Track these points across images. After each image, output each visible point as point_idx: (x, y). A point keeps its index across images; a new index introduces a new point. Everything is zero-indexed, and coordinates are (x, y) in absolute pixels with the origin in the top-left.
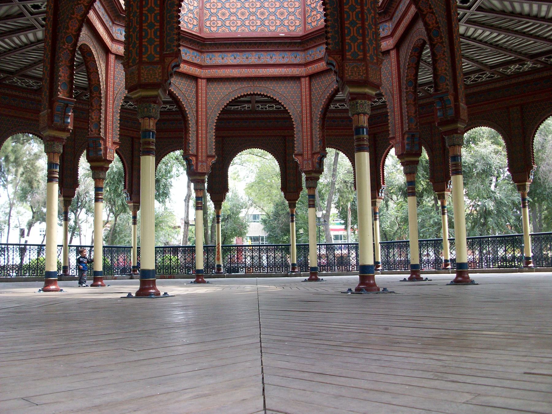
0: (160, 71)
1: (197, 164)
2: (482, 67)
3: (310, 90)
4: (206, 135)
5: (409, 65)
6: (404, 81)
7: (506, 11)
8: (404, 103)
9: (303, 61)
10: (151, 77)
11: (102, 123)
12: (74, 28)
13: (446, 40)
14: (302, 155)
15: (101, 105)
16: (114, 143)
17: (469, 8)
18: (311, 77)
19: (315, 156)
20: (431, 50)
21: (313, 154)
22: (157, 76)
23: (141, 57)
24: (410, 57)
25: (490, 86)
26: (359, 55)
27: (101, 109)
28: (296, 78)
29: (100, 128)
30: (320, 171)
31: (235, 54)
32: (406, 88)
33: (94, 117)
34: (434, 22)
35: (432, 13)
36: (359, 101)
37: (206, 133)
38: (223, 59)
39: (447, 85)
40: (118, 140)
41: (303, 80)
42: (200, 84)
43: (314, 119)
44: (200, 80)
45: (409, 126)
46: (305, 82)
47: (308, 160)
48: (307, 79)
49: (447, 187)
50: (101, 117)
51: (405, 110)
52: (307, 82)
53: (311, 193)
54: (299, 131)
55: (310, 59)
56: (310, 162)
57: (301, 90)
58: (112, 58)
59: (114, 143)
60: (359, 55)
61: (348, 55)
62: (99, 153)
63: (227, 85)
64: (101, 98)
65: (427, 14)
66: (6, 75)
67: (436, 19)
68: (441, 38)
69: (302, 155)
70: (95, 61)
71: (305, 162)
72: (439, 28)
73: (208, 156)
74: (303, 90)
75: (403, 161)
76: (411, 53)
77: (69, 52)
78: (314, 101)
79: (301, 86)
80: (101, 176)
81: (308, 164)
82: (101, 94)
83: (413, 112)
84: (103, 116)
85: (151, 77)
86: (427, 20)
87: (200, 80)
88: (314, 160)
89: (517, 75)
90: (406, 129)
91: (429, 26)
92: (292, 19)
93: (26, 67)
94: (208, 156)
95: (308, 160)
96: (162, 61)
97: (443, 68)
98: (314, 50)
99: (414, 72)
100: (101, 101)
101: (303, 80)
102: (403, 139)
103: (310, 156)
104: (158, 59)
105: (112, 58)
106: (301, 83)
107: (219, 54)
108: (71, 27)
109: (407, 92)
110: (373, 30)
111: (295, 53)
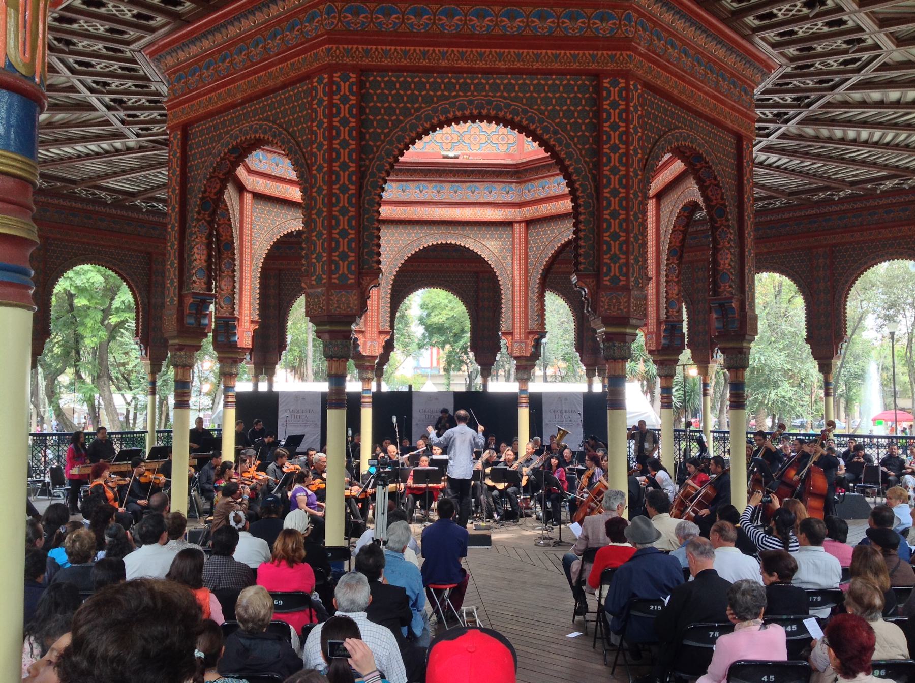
0: (355, 298)
1: (365, 344)
2: (777, 191)
3: (527, 242)
4: (378, 302)
5: (674, 226)
6: (665, 247)
7: (822, 136)
8: (663, 279)
9: (517, 200)
11: (237, 296)
12: (213, 191)
13: (733, 222)
14: (511, 334)
15: (234, 271)
16: (252, 322)
17: (768, 135)
19: (531, 337)
20: (708, 213)
23: (330, 278)
24: (677, 217)
25: (786, 215)
26: (620, 280)
27: (234, 276)
28: (508, 224)
29: (234, 304)
30: (536, 355)
31: (421, 185)
32: (668, 260)
33: (223, 287)
34: (719, 197)
35: (717, 185)
36: (617, 344)
37: (378, 298)
38: (404, 191)
39: (730, 286)
40: (257, 318)
43: (531, 284)
45: (668, 312)
46: (519, 229)
48: (523, 224)
49: (712, 357)
50: (234, 287)
51: (663, 289)
52: (523, 230)
55: (529, 197)
57: (513, 239)
58: (248, 197)
59: (252, 322)
60: (620, 280)
61: (606, 281)
62: (232, 339)
63: (409, 229)
64: (234, 260)
65: (709, 186)
66: (63, 184)
67: (723, 194)
68: (728, 220)
69: (511, 334)
70: (227, 210)
71: (516, 345)
72: (724, 205)
73: (381, 333)
74: (517, 241)
75: (659, 358)
76: (680, 213)
77: (206, 224)
78: (532, 259)
79: (513, 234)
80: (234, 371)
82: (234, 254)
83: (675, 292)
84: (237, 285)
86: (710, 194)
88: (529, 342)
89: (828, 202)
90: (663, 316)
91: (716, 222)
93: (99, 177)
94: (381, 333)
96: (359, 284)
97: (727, 262)
98: (536, 183)
99: (681, 237)
100: (235, 265)
101: (516, 226)
103: (523, 336)
104: (353, 281)
105: (248, 197)
106: (513, 231)
107: (398, 184)
108: (209, 190)
109: (667, 265)
110: (640, 242)
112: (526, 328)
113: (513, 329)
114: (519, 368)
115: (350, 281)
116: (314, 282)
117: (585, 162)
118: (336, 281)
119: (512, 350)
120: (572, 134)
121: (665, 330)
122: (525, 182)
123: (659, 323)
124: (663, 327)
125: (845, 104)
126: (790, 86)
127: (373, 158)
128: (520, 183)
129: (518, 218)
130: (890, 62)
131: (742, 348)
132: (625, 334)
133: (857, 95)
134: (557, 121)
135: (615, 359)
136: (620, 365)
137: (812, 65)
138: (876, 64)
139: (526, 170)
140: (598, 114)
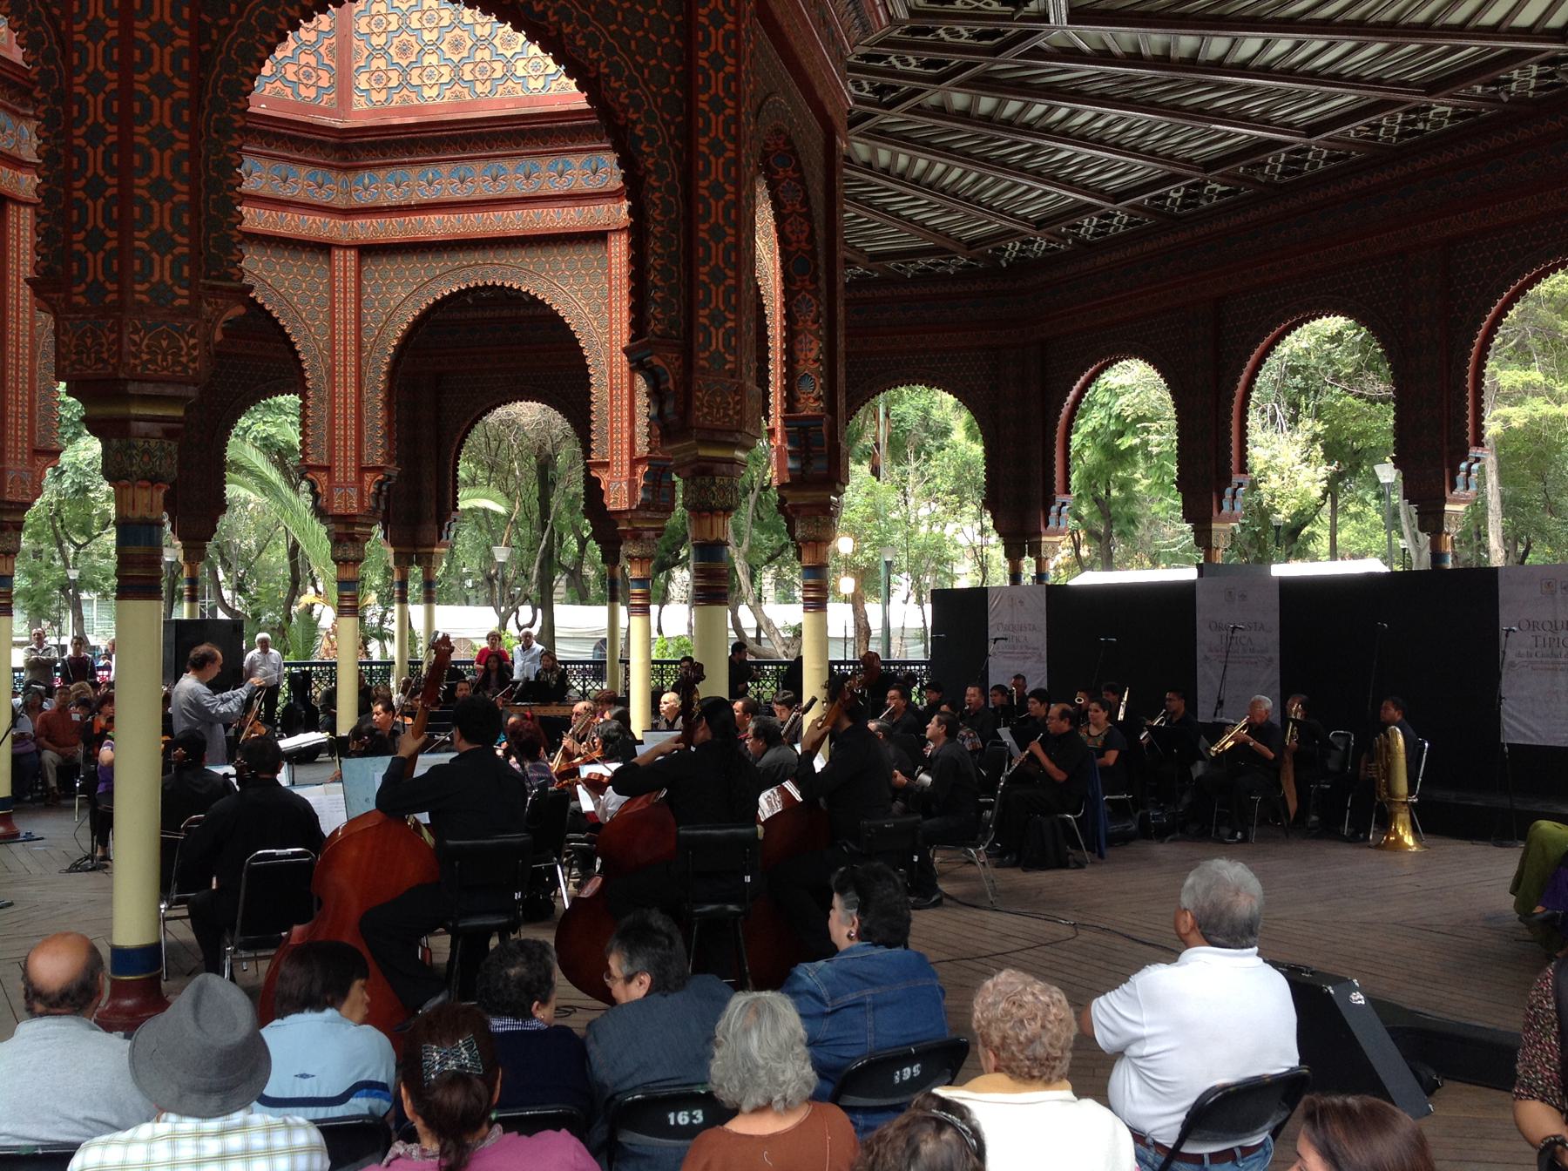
9: (341, 202)
10: (165, 359)
14: (328, 469)
18: (368, 251)
19: (368, 477)
21: (362, 470)
22: (184, 360)
28: (323, 248)
41: (338, 254)
42: (13, 219)
43: (369, 374)
44: (12, 207)
46: (345, 261)
47: (345, 485)
48: (351, 254)
53: (349, 574)
54: (322, 400)
55: (365, 199)
56: (353, 492)
69: (328, 469)
71: (337, 493)
81: (346, 498)
85: (165, 359)
87: (12, 207)
90: (642, 449)
92: (308, 65)
95: (345, 485)
98: (382, 172)
101: (338, 254)
102: (633, 472)
103: (352, 476)
111: (320, 174)
112: (359, 456)
113: (332, 457)
114: (337, 540)
115: (177, 303)
116: (80, 300)
117: (663, 119)
118: (143, 297)
119: (330, 500)
120: (641, 61)
121: (646, 476)
122: (356, 168)
123: (634, 463)
124: (642, 470)
125: (941, 111)
126: (882, 64)
127: (230, 27)
128: (346, 170)
129: (346, 239)
130: (1045, 45)
131: (830, 503)
132: (733, 461)
133: (959, 100)
134: (613, 27)
135: (713, 511)
136: (720, 521)
137: (933, 31)
138: (1024, 47)
139: (362, 146)
140: (688, 30)
